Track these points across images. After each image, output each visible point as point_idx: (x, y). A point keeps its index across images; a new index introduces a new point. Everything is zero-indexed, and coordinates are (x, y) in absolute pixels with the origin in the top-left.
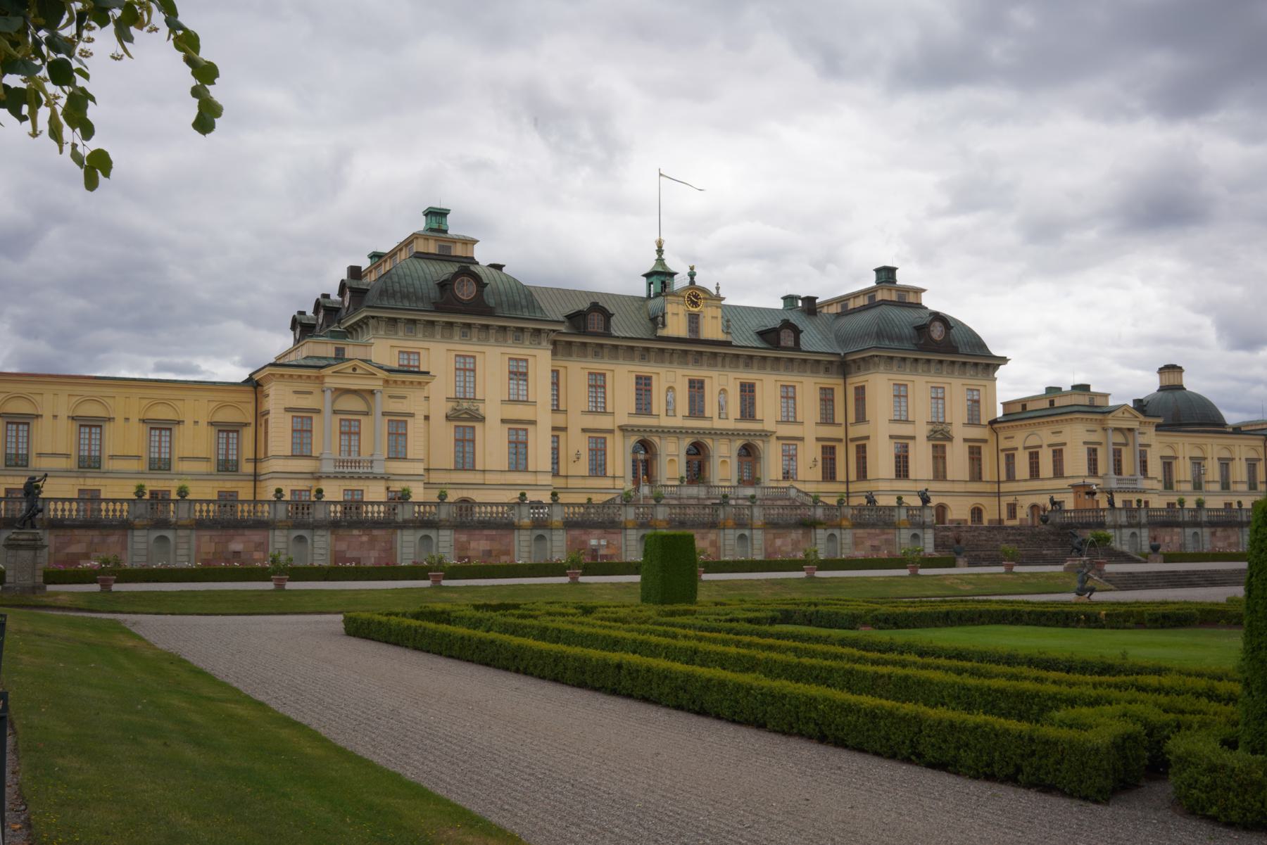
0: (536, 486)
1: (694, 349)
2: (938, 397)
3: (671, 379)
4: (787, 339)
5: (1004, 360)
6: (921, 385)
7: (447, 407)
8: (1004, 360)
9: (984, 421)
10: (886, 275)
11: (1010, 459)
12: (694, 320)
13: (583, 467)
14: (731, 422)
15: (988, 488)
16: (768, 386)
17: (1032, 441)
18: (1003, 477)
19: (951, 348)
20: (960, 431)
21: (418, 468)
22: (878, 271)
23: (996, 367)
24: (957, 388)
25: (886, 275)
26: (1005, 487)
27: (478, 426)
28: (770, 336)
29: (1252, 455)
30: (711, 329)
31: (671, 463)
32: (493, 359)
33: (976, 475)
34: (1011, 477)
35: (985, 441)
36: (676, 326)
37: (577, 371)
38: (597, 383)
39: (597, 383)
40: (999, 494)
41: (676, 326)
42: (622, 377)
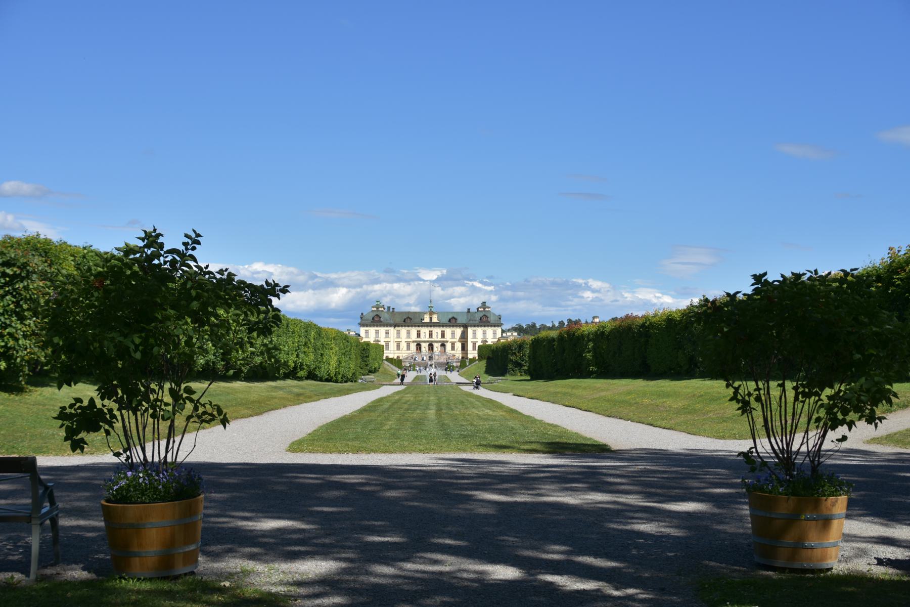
1: (431, 324)
2: (484, 333)
3: (425, 331)
4: (453, 321)
6: (480, 330)
12: (431, 319)
13: (405, 348)
14: (439, 339)
16: (448, 331)
28: (450, 321)
30: (435, 319)
31: (425, 347)
32: (382, 330)
36: (427, 319)
37: (403, 330)
38: (408, 332)
39: (408, 332)
41: (427, 319)
42: (414, 331)
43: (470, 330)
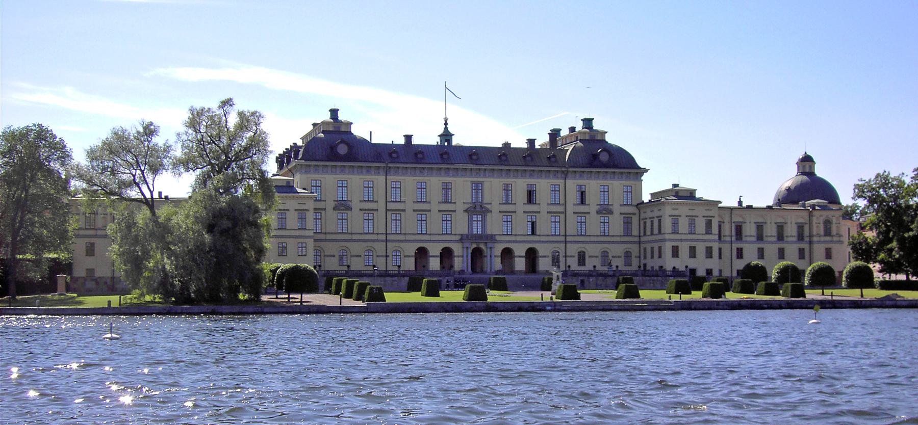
0: (378, 241)
5: (646, 171)
7: (333, 204)
8: (646, 171)
9: (635, 203)
10: (588, 122)
11: (645, 223)
15: (636, 239)
17: (651, 215)
18: (642, 234)
19: (622, 164)
20: (617, 209)
21: (311, 233)
22: (583, 120)
23: (642, 174)
24: (617, 185)
25: (588, 122)
26: (643, 239)
27: (349, 212)
29: (801, 220)
33: (627, 232)
34: (645, 235)
35: (635, 214)
40: (640, 242)
43: (572, 185)
